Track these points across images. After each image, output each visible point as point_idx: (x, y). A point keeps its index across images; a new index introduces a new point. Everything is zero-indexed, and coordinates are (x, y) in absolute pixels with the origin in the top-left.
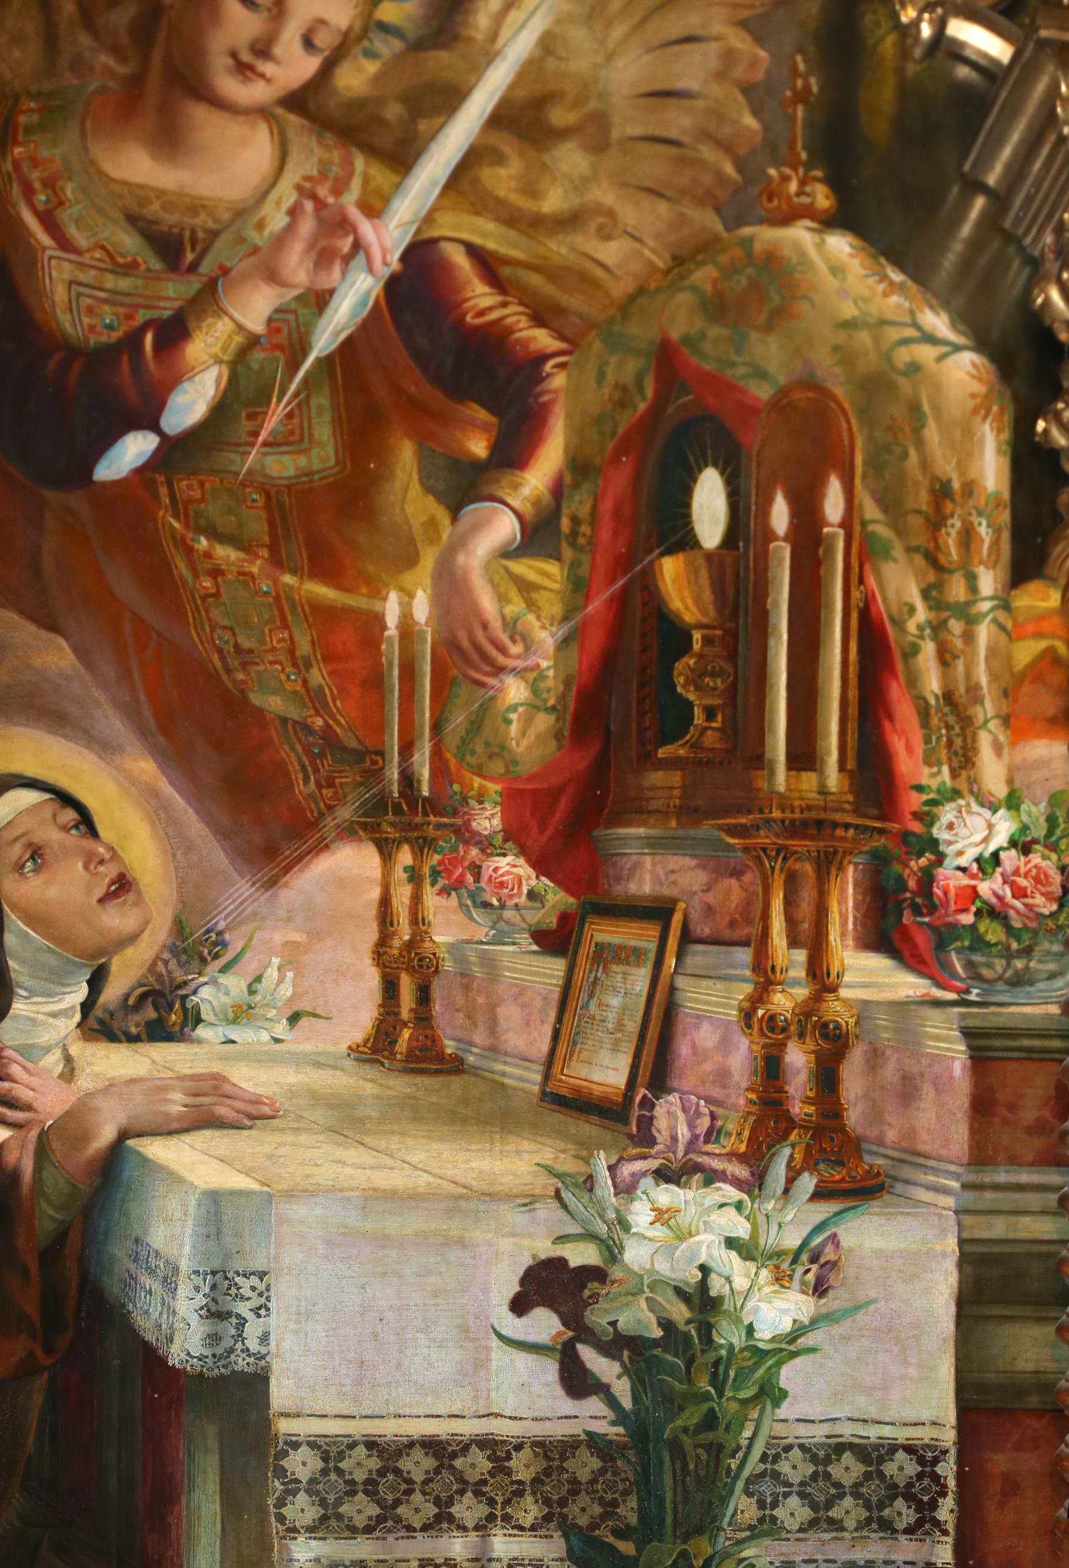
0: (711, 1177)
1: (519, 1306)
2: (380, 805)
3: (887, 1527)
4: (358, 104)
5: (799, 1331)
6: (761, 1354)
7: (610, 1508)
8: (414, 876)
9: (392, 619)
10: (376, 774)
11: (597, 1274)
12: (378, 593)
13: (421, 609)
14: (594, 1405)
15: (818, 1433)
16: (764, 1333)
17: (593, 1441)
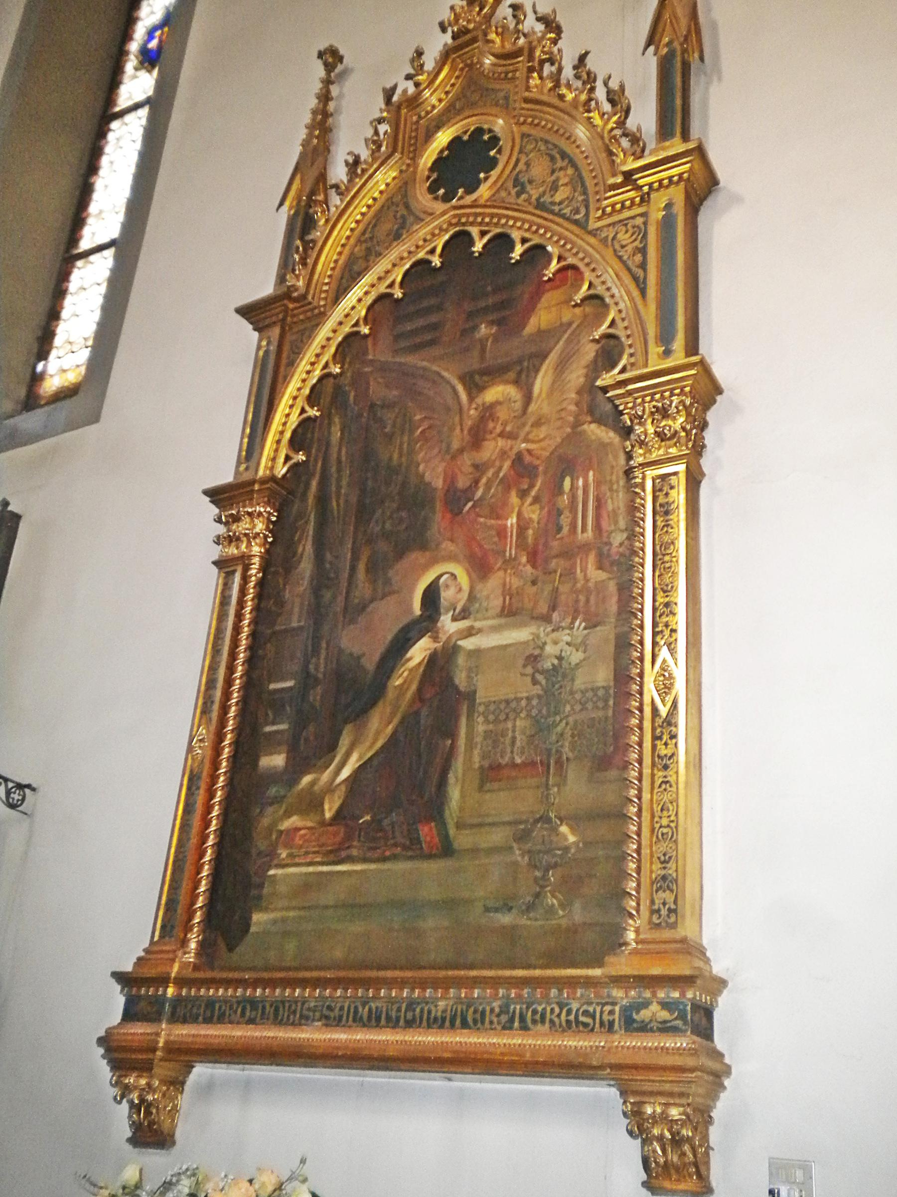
0: (563, 629)
1: (525, 666)
2: (505, 562)
3: (597, 708)
4: (509, 432)
5: (581, 661)
6: (572, 669)
7: (540, 711)
8: (510, 575)
9: (509, 525)
10: (504, 556)
11: (540, 655)
12: (507, 519)
13: (515, 520)
14: (538, 687)
15: (583, 687)
16: (573, 663)
17: (539, 697)
